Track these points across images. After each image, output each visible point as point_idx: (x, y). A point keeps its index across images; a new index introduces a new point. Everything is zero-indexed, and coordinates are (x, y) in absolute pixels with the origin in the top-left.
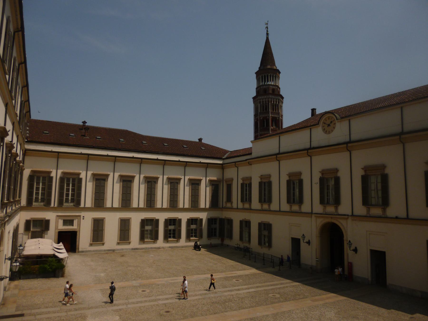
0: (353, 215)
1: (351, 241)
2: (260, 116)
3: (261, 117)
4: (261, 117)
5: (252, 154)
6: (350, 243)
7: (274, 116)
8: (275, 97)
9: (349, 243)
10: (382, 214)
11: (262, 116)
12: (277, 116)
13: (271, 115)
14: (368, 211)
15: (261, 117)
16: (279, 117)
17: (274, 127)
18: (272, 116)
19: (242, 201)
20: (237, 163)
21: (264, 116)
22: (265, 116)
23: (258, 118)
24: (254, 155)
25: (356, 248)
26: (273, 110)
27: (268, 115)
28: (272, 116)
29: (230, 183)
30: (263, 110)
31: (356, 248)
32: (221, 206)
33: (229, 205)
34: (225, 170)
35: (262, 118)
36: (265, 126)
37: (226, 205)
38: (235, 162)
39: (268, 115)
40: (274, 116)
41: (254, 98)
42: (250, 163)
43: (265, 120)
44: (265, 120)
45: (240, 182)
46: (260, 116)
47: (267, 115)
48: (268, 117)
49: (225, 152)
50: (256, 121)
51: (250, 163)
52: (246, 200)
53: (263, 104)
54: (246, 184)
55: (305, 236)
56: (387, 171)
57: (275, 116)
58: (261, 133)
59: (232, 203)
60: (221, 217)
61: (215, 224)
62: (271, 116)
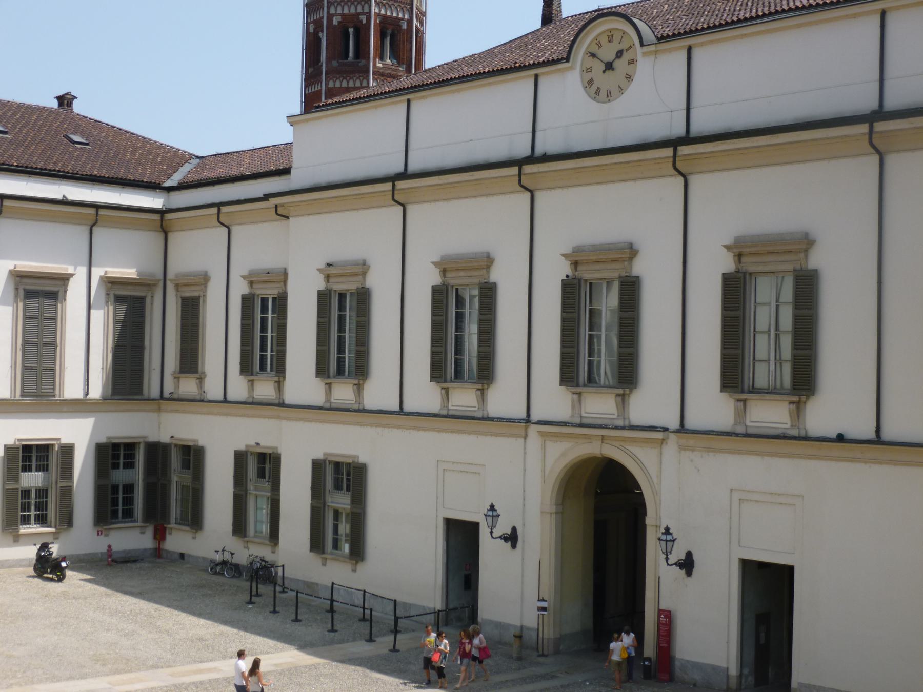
0: (682, 429)
1: (671, 531)
2: (332, 11)
3: (333, 15)
4: (336, 15)
5: (292, 171)
6: (669, 537)
7: (389, 13)
9: (664, 537)
10: (788, 426)
11: (339, 11)
12: (400, 16)
13: (377, 11)
14: (741, 412)
15: (336, 15)
16: (410, 22)
17: (388, 61)
18: (383, 12)
19: (246, 368)
20: (224, 209)
21: (346, 11)
22: (353, 11)
23: (322, 18)
24: (296, 180)
25: (689, 554)
27: (366, 10)
29: (196, 294)
31: (689, 554)
32: (155, 392)
33: (188, 386)
34: (173, 238)
35: (339, 18)
36: (351, 54)
37: (177, 386)
38: (219, 205)
39: (366, 10)
40: (391, 17)
42: (280, 211)
43: (351, 30)
44: (351, 30)
45: (240, 288)
46: (332, 11)
47: (359, 10)
48: (364, 19)
49: (178, 158)
50: (311, 30)
51: (280, 211)
52: (263, 367)
54: (264, 301)
55: (499, 512)
56: (816, 260)
57: (395, 15)
58: (331, 84)
59: (201, 380)
60: (153, 438)
61: (130, 465)
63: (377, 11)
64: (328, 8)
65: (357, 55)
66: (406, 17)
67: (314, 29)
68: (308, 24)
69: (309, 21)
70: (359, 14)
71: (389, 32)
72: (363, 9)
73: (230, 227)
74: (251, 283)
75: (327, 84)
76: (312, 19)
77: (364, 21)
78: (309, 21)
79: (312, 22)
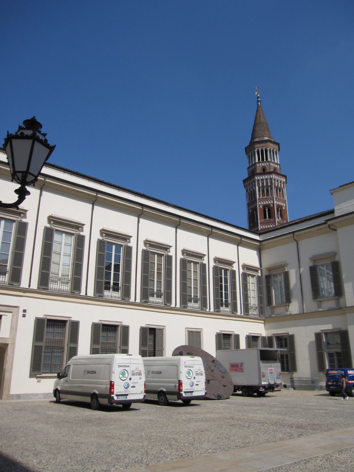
3: (260, 205)
5: (335, 211)
7: (279, 204)
8: (279, 179)
11: (262, 203)
12: (283, 205)
13: (276, 203)
18: (277, 203)
20: (296, 234)
21: (265, 203)
22: (267, 203)
24: (337, 214)
26: (277, 196)
28: (277, 204)
30: (263, 195)
38: (293, 233)
41: (245, 181)
42: (330, 227)
43: (267, 209)
44: (267, 209)
47: (269, 202)
50: (250, 211)
51: (332, 227)
53: (263, 186)
57: (281, 204)
62: (276, 204)
63: (276, 203)
64: (258, 202)
65: (269, 217)
66: (284, 205)
67: (252, 211)
68: (249, 210)
69: (249, 209)
70: (270, 204)
71: (279, 210)
72: (271, 202)
73: (298, 242)
74: (314, 261)
75: (260, 227)
76: (251, 208)
77: (272, 206)
78: (249, 209)
79: (250, 209)
